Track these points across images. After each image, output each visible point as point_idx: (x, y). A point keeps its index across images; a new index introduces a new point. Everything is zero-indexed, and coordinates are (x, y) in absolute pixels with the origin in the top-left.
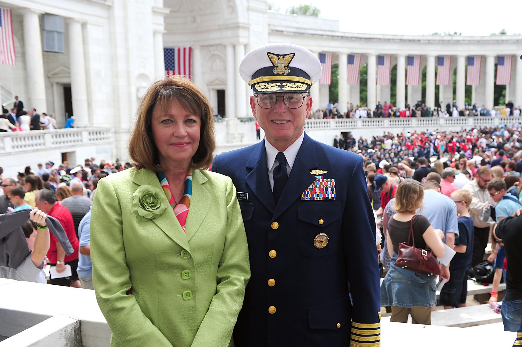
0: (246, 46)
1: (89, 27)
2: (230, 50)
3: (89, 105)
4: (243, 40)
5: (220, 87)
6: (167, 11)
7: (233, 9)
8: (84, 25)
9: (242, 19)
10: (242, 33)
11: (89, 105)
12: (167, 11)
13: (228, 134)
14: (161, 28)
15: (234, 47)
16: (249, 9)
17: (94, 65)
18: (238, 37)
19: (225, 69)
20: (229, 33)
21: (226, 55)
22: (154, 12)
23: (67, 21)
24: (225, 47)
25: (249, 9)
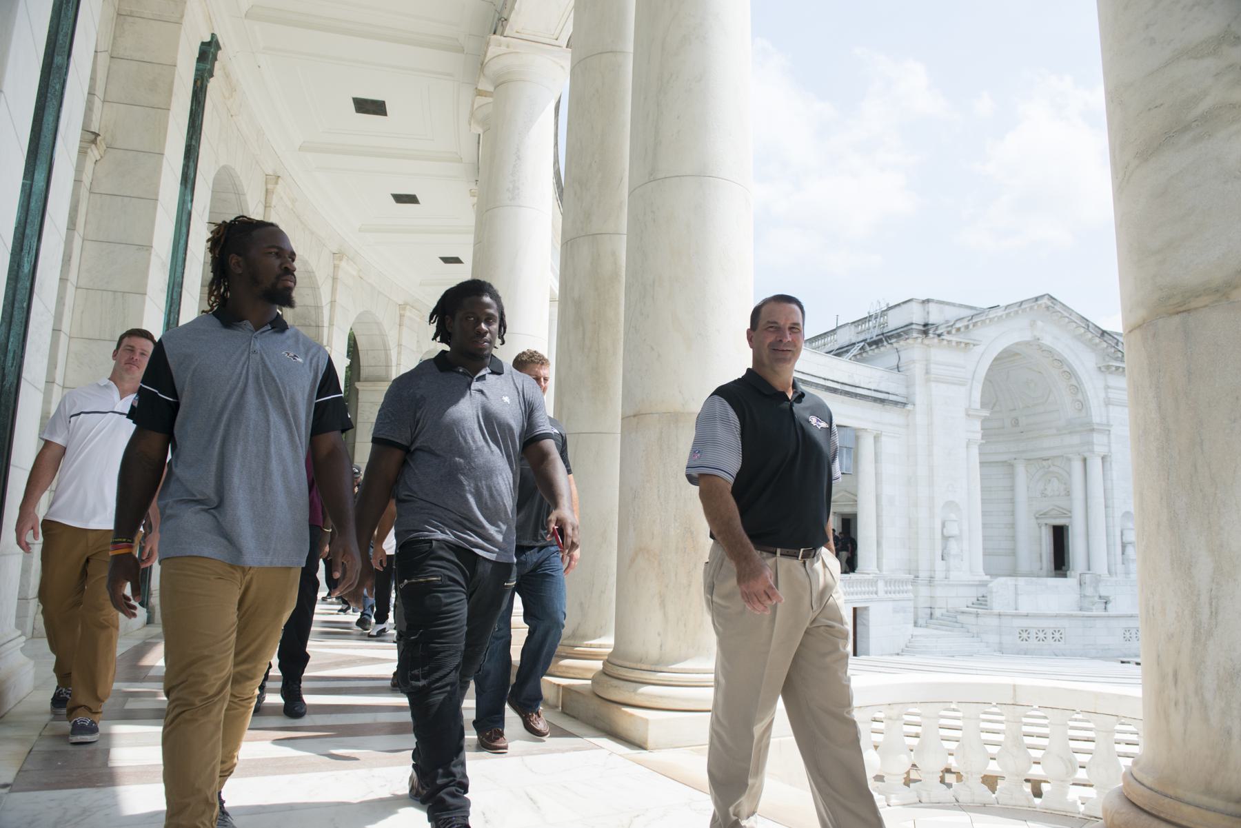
0: (1103, 458)
1: (883, 439)
2: (1077, 466)
3: (879, 544)
4: (1100, 449)
5: (1059, 522)
6: (986, 413)
7: (1083, 405)
8: (877, 438)
9: (1096, 419)
10: (1097, 438)
11: (879, 544)
12: (986, 413)
13: (1083, 596)
14: (979, 436)
15: (1085, 460)
16: (1108, 403)
17: (887, 490)
18: (1091, 443)
19: (1068, 494)
20: (1076, 439)
21: (1070, 474)
22: (968, 415)
23: (856, 434)
24: (1069, 460)
25: (1108, 403)
